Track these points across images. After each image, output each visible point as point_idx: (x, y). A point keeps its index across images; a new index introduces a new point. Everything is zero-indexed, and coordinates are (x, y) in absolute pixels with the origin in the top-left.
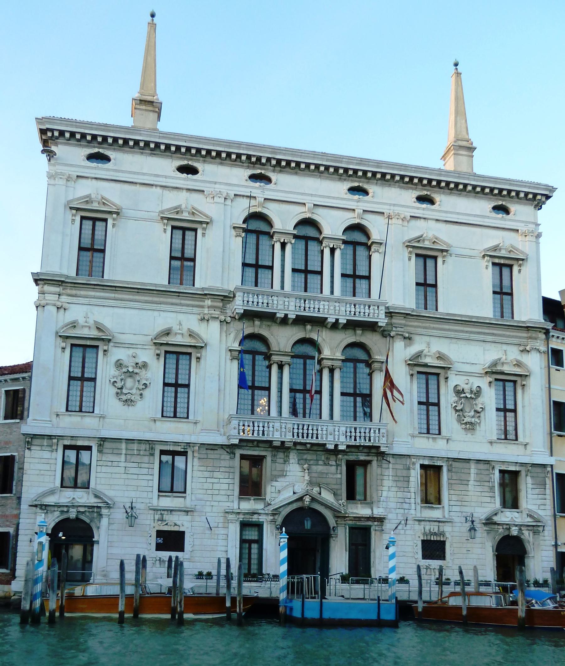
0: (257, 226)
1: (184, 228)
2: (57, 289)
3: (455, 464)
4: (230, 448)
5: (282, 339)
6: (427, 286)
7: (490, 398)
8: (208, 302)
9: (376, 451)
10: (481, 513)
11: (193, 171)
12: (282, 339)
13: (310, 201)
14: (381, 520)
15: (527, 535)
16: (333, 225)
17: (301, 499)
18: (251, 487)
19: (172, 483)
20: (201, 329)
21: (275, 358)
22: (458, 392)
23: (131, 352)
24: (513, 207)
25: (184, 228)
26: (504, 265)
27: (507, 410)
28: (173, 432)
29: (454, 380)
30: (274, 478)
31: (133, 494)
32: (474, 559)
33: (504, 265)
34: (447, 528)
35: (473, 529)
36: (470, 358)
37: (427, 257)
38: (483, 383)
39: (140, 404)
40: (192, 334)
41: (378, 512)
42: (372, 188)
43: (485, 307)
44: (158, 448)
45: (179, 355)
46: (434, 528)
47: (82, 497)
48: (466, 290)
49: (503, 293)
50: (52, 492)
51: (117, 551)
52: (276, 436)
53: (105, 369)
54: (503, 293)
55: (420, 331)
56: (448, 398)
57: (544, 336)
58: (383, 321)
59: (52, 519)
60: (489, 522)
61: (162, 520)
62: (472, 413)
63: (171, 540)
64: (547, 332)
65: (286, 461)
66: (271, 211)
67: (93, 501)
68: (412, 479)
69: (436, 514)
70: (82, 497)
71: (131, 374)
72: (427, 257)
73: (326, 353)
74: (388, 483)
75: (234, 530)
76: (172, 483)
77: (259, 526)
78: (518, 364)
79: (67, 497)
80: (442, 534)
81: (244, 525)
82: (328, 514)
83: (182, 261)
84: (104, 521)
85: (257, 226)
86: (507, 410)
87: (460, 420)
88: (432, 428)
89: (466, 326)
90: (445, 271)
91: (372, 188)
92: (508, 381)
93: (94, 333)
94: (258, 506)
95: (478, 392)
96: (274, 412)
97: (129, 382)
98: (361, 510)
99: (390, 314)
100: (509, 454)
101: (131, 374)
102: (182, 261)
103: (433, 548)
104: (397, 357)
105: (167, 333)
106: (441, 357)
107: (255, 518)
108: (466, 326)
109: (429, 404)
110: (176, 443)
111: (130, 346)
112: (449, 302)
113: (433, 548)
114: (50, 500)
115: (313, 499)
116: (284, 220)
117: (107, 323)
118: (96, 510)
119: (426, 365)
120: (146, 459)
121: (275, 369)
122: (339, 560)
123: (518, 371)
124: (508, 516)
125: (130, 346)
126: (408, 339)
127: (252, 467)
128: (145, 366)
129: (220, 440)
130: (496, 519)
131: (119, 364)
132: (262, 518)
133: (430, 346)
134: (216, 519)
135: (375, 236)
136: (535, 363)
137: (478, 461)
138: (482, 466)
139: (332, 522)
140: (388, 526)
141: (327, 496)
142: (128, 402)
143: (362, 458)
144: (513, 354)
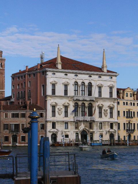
0: (76, 83)
1: (66, 86)
2: (50, 97)
3: (104, 122)
4: (74, 122)
5: (80, 103)
6: (100, 92)
7: (109, 111)
8: (70, 98)
9: (94, 121)
10: (108, 130)
11: (67, 75)
12: (80, 103)
13: (83, 79)
14: (94, 132)
15: (114, 133)
16: (87, 84)
17: (84, 129)
18: (77, 128)
19: (67, 128)
20: (69, 102)
21: (79, 106)
22: (104, 110)
23: (60, 107)
24: (113, 77)
25: (66, 86)
26: (111, 88)
27: (111, 113)
28: (66, 119)
29: (104, 108)
30: (80, 126)
31: (62, 129)
32: (107, 137)
33: (111, 88)
34: (103, 133)
35: (107, 133)
36: (106, 104)
37: (100, 88)
38: (108, 108)
39: (61, 115)
40: (68, 103)
41: (94, 131)
42: (92, 76)
43: (108, 96)
44: (64, 122)
45: (66, 107)
46: (101, 133)
47: (55, 130)
48: (105, 93)
49: (111, 93)
50: (51, 130)
51: (59, 139)
52: (81, 120)
53: (57, 110)
54: (111, 93)
55: (100, 100)
56: (103, 111)
57: (117, 100)
58: (94, 99)
59: (52, 133)
60: (109, 131)
61: (65, 133)
62: (106, 114)
63: (67, 136)
64: (117, 99)
65: (81, 123)
66: (78, 81)
67: (56, 131)
68: (98, 125)
69: (101, 130)
70: (55, 130)
71: (60, 110)
72: (100, 88)
73: (86, 105)
74: (95, 126)
75: (75, 134)
76: (67, 128)
77: (78, 133)
78: (113, 105)
79: (53, 130)
80: (102, 133)
81: (76, 133)
82: (87, 131)
83: (66, 92)
84: (58, 133)
85: (76, 83)
86: (111, 113)
87: (104, 115)
88: (100, 116)
89: (105, 99)
90: (103, 89)
91: (92, 76)
92: (111, 109)
93: (55, 104)
94: (78, 130)
95: (107, 110)
96: (79, 116)
97: (60, 112)
98: (91, 130)
99: (95, 98)
100: (112, 120)
101: (60, 110)
102: (66, 92)
103: (102, 136)
104: (96, 105)
105: (64, 104)
106: (102, 105)
107: (77, 132)
108: (105, 99)
109: (100, 113)
110: (67, 121)
111: (60, 106)
112: (103, 96)
113: (102, 136)
114: (51, 131)
115: (85, 129)
116: (80, 83)
117: (56, 102)
118: (57, 132)
119: (100, 106)
120: (63, 124)
121: (79, 108)
122: (89, 138)
123: (113, 106)
124: (111, 130)
125: (60, 106)
126: (97, 102)
127: (77, 123)
128: (61, 109)
129: (73, 120)
130: (110, 131)
131: (58, 109)
132: (79, 132)
133: (100, 103)
134: (72, 133)
135: (93, 84)
136: (116, 104)
137: (107, 122)
138: (108, 122)
139: (88, 132)
140: (95, 133)
141: (87, 128)
142: (60, 115)
143: (92, 122)
144: (112, 103)
